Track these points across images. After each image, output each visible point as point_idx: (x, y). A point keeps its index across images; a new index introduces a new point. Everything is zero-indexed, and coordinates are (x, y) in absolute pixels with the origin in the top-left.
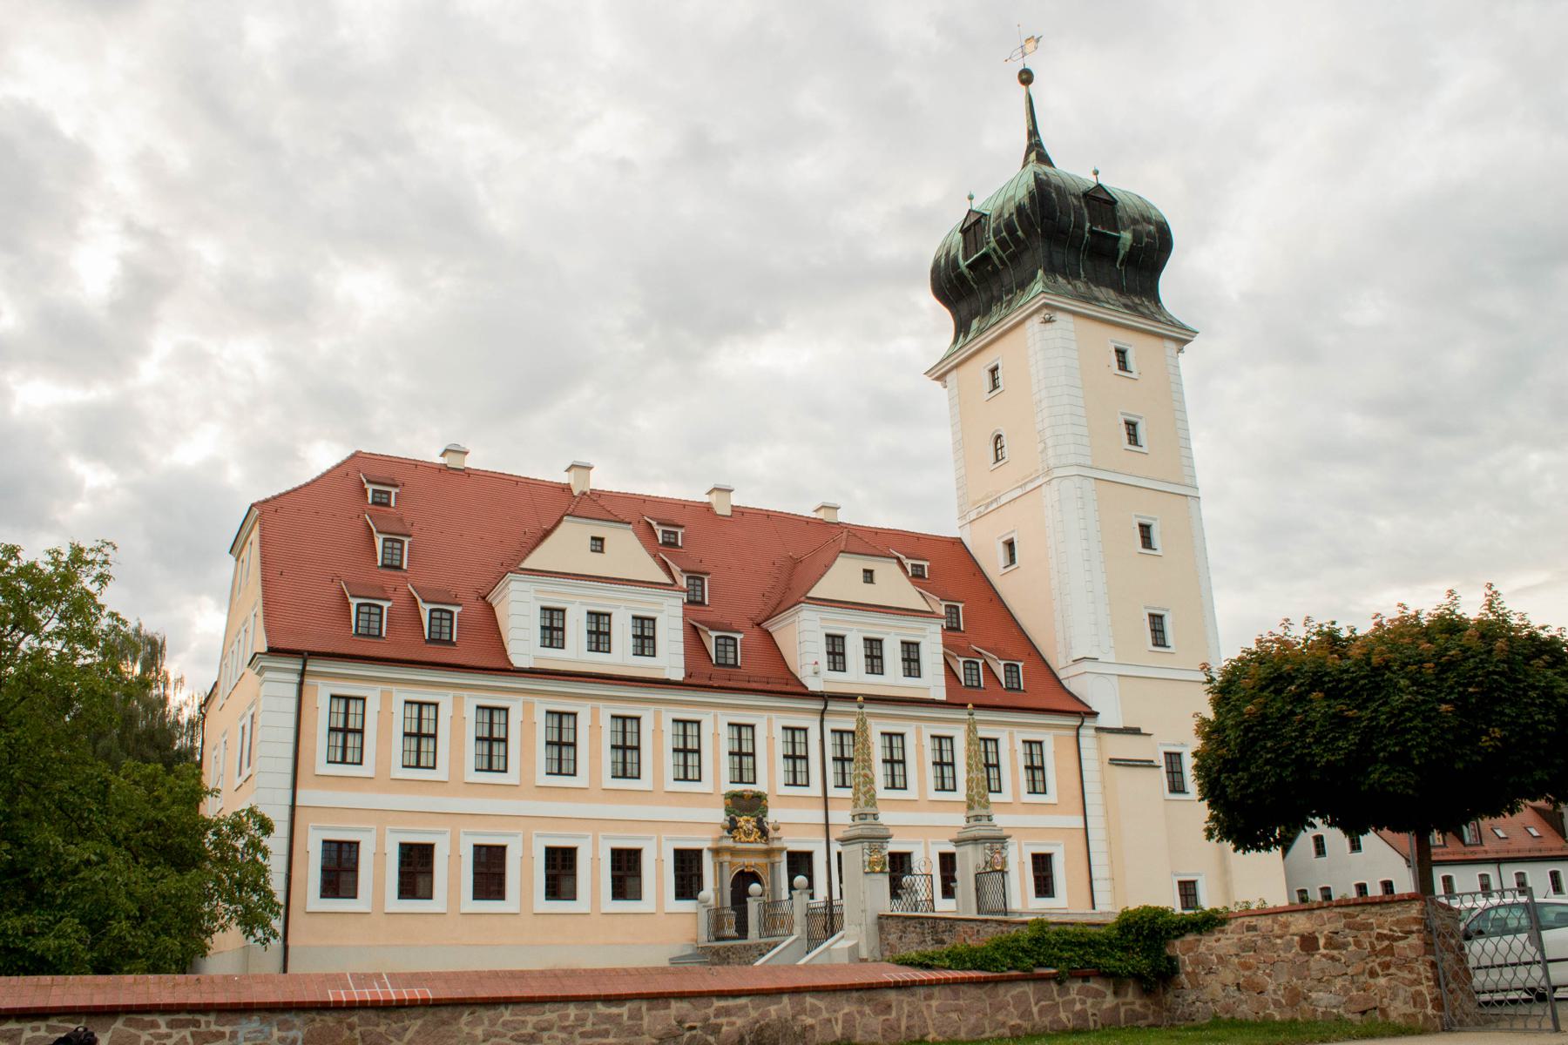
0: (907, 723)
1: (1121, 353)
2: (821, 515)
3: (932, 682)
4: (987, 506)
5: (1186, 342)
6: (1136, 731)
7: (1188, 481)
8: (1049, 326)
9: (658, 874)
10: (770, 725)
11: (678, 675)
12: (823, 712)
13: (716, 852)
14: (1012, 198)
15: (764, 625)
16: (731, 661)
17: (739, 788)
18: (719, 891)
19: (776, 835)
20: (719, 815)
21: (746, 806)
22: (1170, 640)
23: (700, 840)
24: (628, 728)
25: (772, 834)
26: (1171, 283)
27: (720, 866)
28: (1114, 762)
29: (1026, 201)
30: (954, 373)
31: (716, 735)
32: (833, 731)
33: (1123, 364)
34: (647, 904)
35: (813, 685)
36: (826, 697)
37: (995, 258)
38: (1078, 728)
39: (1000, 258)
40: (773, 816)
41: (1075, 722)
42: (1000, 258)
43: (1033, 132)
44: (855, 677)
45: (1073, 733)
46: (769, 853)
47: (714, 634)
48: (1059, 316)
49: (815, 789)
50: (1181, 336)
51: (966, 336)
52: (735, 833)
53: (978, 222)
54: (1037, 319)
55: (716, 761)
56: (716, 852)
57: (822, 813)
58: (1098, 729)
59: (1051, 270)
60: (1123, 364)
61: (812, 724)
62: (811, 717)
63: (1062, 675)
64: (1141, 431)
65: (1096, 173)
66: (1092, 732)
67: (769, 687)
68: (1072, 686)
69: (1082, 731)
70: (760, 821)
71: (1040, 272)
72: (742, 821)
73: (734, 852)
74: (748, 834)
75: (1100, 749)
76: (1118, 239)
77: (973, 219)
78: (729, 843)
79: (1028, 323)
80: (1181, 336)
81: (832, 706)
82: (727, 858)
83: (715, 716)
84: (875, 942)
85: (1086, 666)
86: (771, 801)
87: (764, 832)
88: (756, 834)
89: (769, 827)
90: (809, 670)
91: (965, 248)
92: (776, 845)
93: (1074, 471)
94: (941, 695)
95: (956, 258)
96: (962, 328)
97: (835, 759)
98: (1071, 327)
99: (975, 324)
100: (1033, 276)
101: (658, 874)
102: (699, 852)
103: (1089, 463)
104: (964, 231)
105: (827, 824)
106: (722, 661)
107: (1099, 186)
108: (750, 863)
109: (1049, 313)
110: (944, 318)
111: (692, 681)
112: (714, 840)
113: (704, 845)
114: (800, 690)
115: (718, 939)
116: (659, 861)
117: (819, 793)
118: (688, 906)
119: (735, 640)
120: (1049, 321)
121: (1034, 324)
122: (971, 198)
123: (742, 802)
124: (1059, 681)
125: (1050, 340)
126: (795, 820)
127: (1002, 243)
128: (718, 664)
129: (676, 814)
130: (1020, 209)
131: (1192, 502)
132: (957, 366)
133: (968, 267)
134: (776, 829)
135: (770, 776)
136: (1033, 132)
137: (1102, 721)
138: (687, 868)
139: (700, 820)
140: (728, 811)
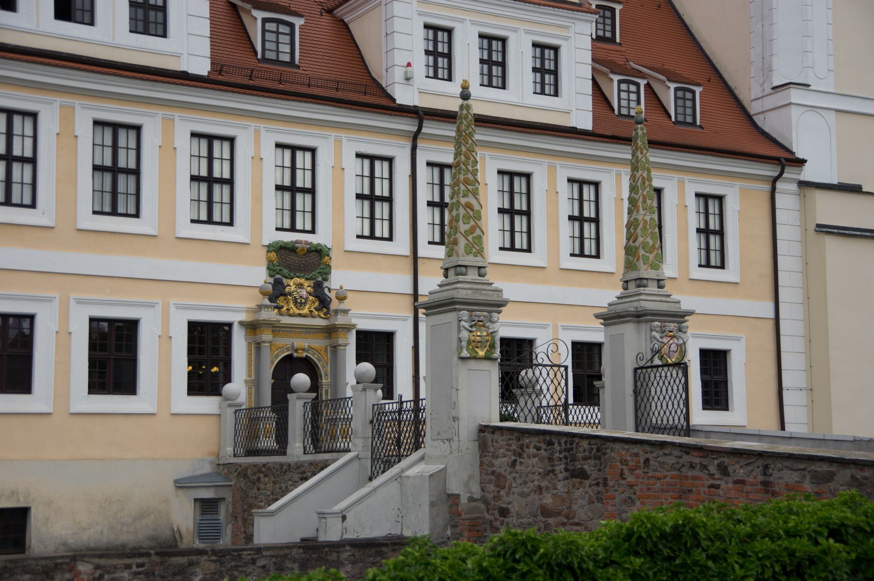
3: (575, 106)
6: (856, 189)
9: (162, 358)
10: (340, 150)
11: (202, 67)
12: (415, 137)
13: (252, 327)
15: (338, 12)
16: (286, 58)
17: (289, 237)
18: (255, 384)
19: (343, 306)
23: (232, 310)
24: (122, 142)
25: (335, 305)
27: (256, 347)
28: (824, 229)
31: (258, 159)
32: (430, 164)
34: (143, 401)
35: (404, 96)
36: (420, 114)
38: (775, 180)
40: (339, 278)
41: (770, 171)
45: (767, 187)
47: (260, 15)
49: (401, 245)
52: (281, 301)
55: (257, 199)
56: (252, 327)
57: (409, 279)
58: (804, 185)
63: (754, 108)
66: (794, 187)
67: (339, 95)
69: (779, 185)
72: (291, 285)
73: (276, 328)
74: (299, 304)
75: (805, 211)
78: (270, 315)
81: (429, 128)
82: (267, 336)
83: (257, 132)
85: (795, 95)
86: (335, 260)
88: (312, 304)
89: (332, 295)
90: (398, 74)
92: (340, 320)
94: (585, 122)
97: (430, 204)
101: (162, 358)
102: (230, 325)
106: (271, 55)
108: (302, 344)
112: (249, 310)
113: (235, 318)
114: (385, 102)
115: (250, 453)
116: (166, 338)
118: (206, 404)
119: (291, 26)
123: (294, 258)
124: (749, 118)
126: (372, 286)
128: (264, 60)
129: (191, 270)
134: (341, 298)
135: (337, 222)
137: (808, 173)
138: (208, 346)
139: (231, 282)
140: (271, 270)
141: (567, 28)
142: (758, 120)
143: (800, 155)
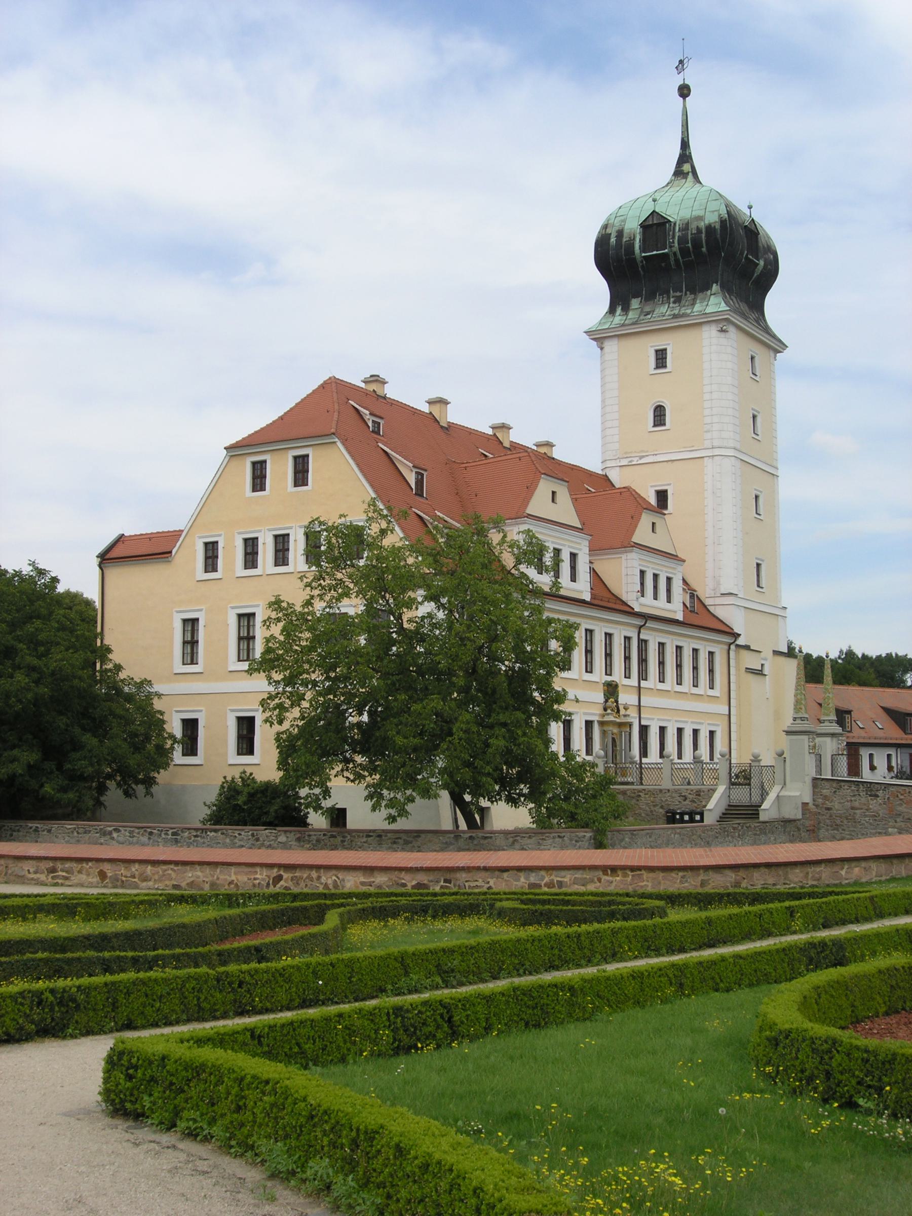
0: (651, 632)
2: (542, 450)
4: (641, 457)
8: (723, 335)
12: (641, 627)
13: (601, 723)
14: (700, 218)
17: (609, 678)
19: (628, 713)
20: (600, 697)
21: (611, 690)
22: (763, 584)
25: (622, 712)
26: (773, 302)
27: (604, 733)
29: (718, 226)
36: (646, 617)
37: (672, 259)
39: (677, 260)
42: (677, 260)
43: (685, 145)
44: (645, 604)
45: (726, 647)
46: (620, 725)
48: (732, 329)
49: (634, 681)
51: (626, 309)
53: (664, 224)
56: (601, 723)
58: (738, 646)
59: (727, 289)
61: (633, 634)
62: (632, 629)
63: (707, 602)
65: (750, 207)
68: (720, 612)
70: (617, 701)
71: (715, 288)
76: (758, 264)
79: (705, 328)
80: (776, 346)
84: (814, 793)
86: (620, 689)
87: (618, 711)
89: (621, 708)
91: (644, 240)
93: (731, 452)
95: (630, 246)
99: (635, 303)
100: (706, 287)
103: (738, 447)
104: (645, 226)
105: (639, 705)
110: (600, 288)
111: (596, 602)
113: (595, 718)
114: (631, 610)
117: (637, 685)
124: (705, 606)
127: (684, 251)
130: (710, 229)
134: (626, 709)
136: (685, 145)
137: (741, 641)
141: (674, 569)
142: (711, 609)
143: (736, 630)
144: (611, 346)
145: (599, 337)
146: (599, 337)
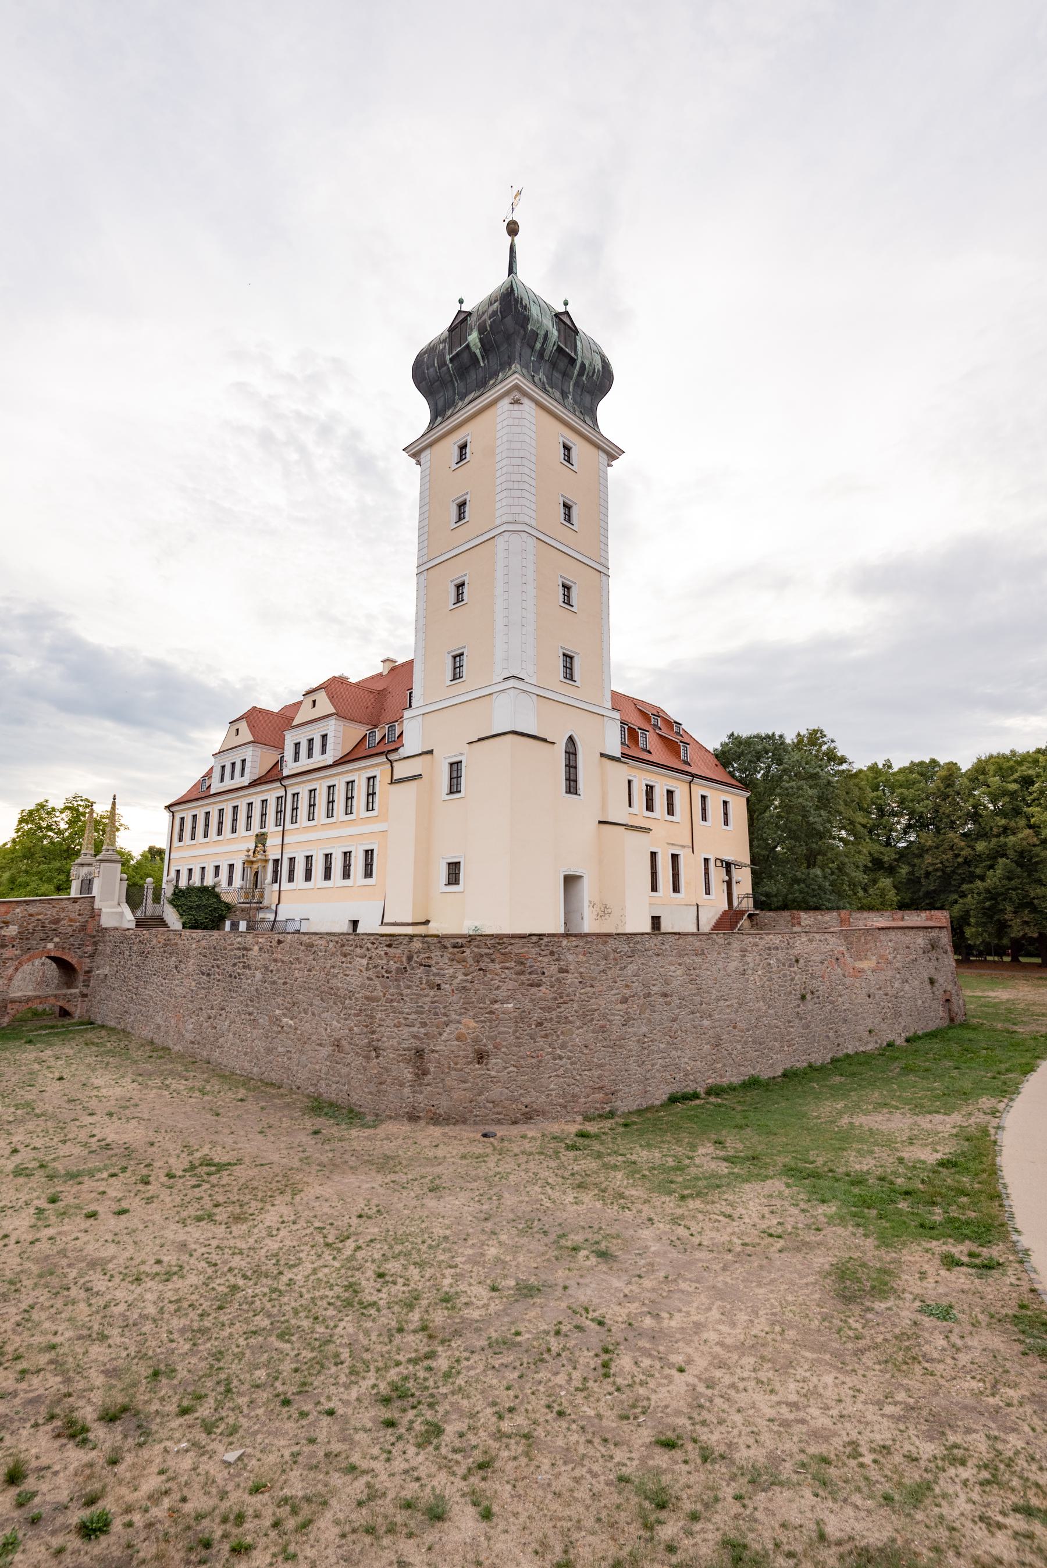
1: (567, 448)
5: (615, 458)
7: (603, 561)
8: (516, 407)
22: (576, 677)
30: (427, 452)
33: (568, 458)
48: (526, 401)
50: (612, 453)
53: (465, 320)
54: (506, 401)
60: (568, 458)
64: (575, 512)
65: (566, 304)
77: (462, 316)
96: (438, 413)
98: (533, 413)
103: (533, 523)
107: (567, 313)
109: (517, 395)
120: (516, 402)
121: (505, 403)
122: (461, 302)
125: (513, 421)
131: (604, 578)
132: (431, 445)
133: (451, 360)
144: (425, 456)
145: (415, 452)
146: (415, 452)
